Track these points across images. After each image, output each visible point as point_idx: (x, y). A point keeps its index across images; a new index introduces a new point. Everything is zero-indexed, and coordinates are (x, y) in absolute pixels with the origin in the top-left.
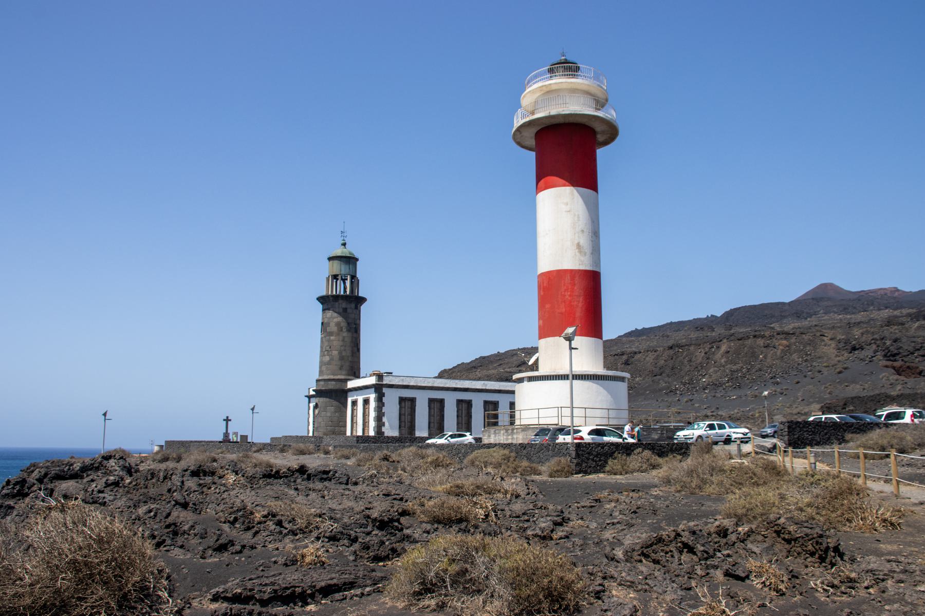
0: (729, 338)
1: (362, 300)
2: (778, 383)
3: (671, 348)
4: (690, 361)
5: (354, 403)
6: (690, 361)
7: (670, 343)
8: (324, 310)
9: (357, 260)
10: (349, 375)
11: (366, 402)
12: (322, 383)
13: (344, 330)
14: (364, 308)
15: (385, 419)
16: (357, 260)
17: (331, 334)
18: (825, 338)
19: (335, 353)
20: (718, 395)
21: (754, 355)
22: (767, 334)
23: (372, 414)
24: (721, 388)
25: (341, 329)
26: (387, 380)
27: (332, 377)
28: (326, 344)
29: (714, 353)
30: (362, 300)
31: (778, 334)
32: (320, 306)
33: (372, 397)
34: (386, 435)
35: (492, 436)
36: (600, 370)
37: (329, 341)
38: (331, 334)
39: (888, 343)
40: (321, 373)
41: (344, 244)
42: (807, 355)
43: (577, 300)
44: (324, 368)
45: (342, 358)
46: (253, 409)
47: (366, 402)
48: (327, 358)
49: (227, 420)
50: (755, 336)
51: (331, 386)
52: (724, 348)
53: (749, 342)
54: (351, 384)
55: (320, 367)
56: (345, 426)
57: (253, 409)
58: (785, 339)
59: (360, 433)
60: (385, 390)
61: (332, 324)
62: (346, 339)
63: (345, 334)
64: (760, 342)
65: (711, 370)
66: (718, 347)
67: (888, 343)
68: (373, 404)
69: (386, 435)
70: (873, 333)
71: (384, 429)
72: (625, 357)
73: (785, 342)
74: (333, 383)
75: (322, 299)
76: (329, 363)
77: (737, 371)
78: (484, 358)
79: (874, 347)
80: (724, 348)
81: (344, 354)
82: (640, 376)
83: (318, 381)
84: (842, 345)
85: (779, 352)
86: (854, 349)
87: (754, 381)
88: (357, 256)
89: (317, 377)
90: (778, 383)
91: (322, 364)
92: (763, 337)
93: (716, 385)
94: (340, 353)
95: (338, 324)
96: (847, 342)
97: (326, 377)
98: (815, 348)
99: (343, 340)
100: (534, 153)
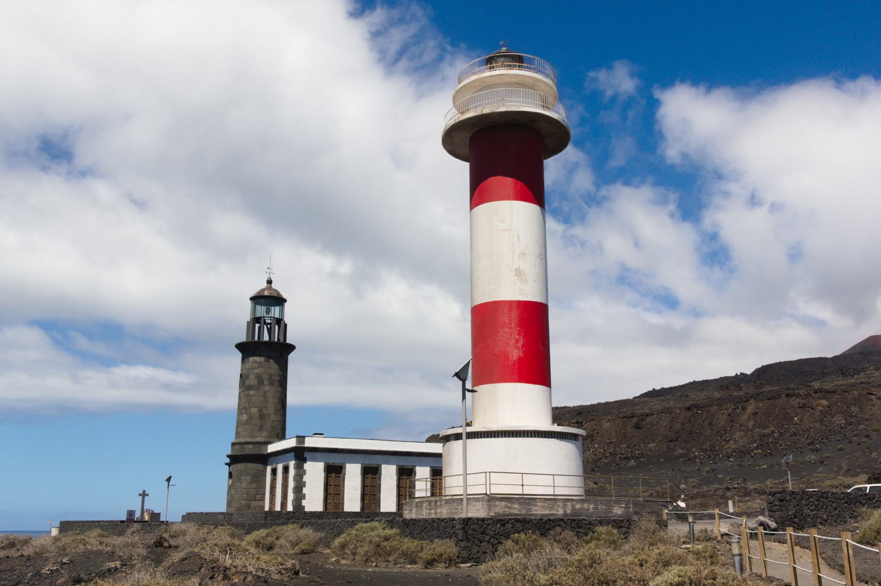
0: (757, 397)
1: (292, 348)
2: (817, 450)
3: (689, 409)
4: (711, 424)
5: (274, 471)
6: (711, 424)
7: (688, 404)
8: (243, 359)
9: (285, 301)
10: (270, 437)
11: (286, 469)
12: (237, 447)
13: (266, 382)
14: (291, 357)
15: (305, 490)
16: (285, 301)
17: (250, 388)
18: (873, 397)
19: (254, 410)
21: (788, 418)
22: (802, 392)
23: (291, 484)
24: (748, 456)
25: (261, 382)
26: (309, 442)
27: (249, 440)
28: (244, 400)
29: (739, 415)
30: (292, 348)
31: (816, 392)
32: (239, 355)
33: (292, 464)
34: (306, 510)
35: (414, 510)
36: (546, 424)
37: (247, 396)
38: (250, 388)
40: (238, 434)
41: (270, 282)
42: (851, 417)
43: (515, 340)
44: (241, 429)
45: (262, 417)
46: (169, 480)
47: (286, 469)
48: (245, 417)
49: (144, 495)
50: (788, 395)
51: (249, 450)
53: (780, 402)
54: (272, 448)
55: (237, 428)
56: (263, 500)
57: (169, 480)
58: (825, 398)
59: (278, 508)
60: (306, 455)
61: (252, 377)
62: (268, 394)
63: (267, 388)
64: (795, 402)
65: (737, 435)
66: (743, 408)
68: (292, 472)
69: (306, 510)
71: (304, 503)
72: (635, 420)
73: (824, 402)
74: (251, 446)
75: (240, 347)
76: (247, 423)
77: (768, 435)
81: (265, 411)
82: (653, 441)
83: (233, 444)
85: (817, 414)
88: (284, 296)
89: (233, 440)
90: (817, 450)
91: (239, 424)
92: (798, 396)
93: (743, 453)
94: (260, 411)
97: (241, 440)
99: (264, 395)
100: (468, 164)
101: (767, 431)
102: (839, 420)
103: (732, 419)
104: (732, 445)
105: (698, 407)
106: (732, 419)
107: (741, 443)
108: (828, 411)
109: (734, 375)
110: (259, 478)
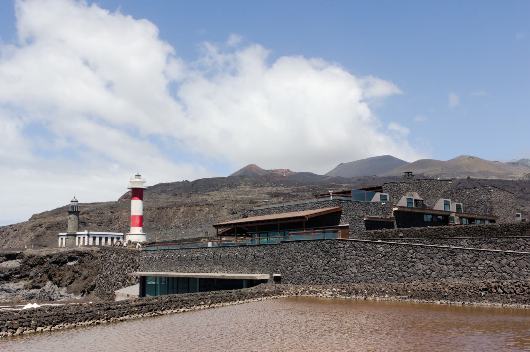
0: (186, 205)
3: (158, 209)
4: (167, 215)
6: (167, 215)
7: (158, 207)
11: (84, 238)
20: (177, 231)
21: (194, 214)
22: (201, 204)
26: (91, 233)
33: (86, 237)
39: (245, 212)
47: (84, 238)
51: (73, 233)
52: (182, 210)
54: (77, 233)
64: (198, 208)
65: (176, 220)
67: (245, 212)
70: (242, 207)
73: (208, 209)
76: (72, 227)
77: (186, 221)
78: (60, 209)
79: (241, 213)
80: (182, 210)
84: (229, 211)
86: (234, 213)
87: (193, 226)
92: (199, 206)
93: (177, 227)
95: (74, 219)
96: (231, 210)
98: (219, 212)
101: (186, 219)
102: (211, 216)
103: (175, 213)
104: (173, 224)
105: (163, 208)
106: (175, 213)
107: (177, 223)
108: (208, 213)
109: (182, 181)
110: (75, 239)
